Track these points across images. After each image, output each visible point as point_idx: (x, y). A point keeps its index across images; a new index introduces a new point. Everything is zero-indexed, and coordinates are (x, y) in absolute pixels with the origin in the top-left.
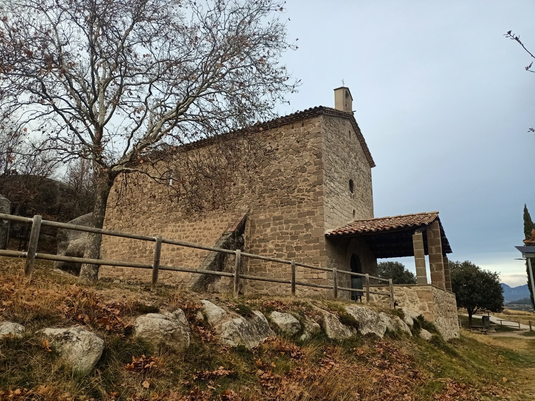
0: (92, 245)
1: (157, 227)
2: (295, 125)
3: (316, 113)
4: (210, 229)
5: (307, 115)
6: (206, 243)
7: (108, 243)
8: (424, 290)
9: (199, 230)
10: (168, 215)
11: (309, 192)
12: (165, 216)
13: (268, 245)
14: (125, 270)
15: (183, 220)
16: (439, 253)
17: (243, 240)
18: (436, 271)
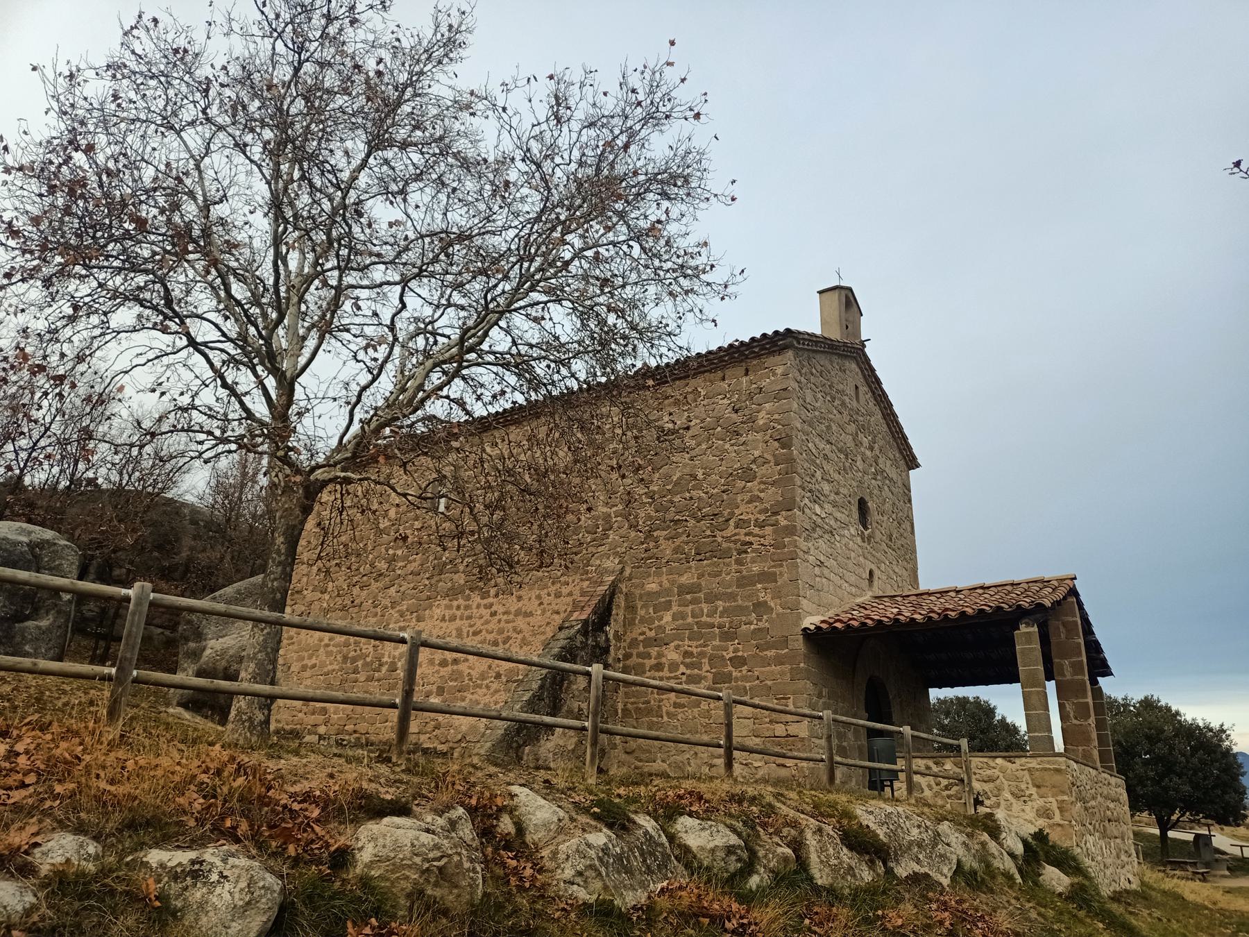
0: (260, 651)
1: (407, 610)
2: (728, 373)
3: (777, 345)
4: (531, 614)
5: (756, 350)
6: (521, 647)
7: (295, 647)
8: (1048, 766)
9: (505, 617)
10: (433, 581)
11: (762, 527)
12: (427, 582)
13: (666, 652)
14: (332, 710)
15: (467, 592)
16: (1080, 677)
17: (607, 640)
18: (1075, 722)
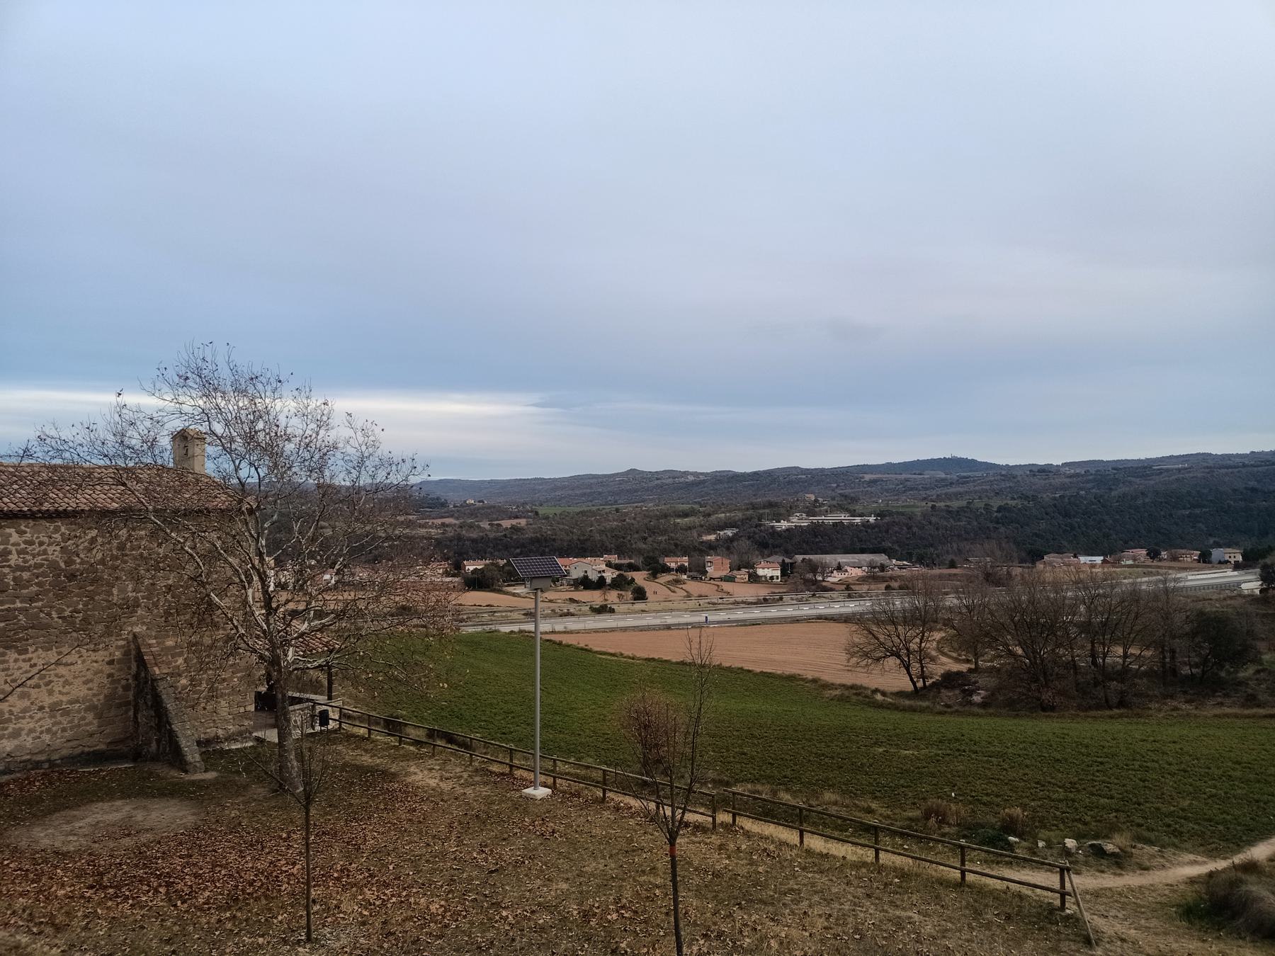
4: (72, 664)
6: (64, 687)
